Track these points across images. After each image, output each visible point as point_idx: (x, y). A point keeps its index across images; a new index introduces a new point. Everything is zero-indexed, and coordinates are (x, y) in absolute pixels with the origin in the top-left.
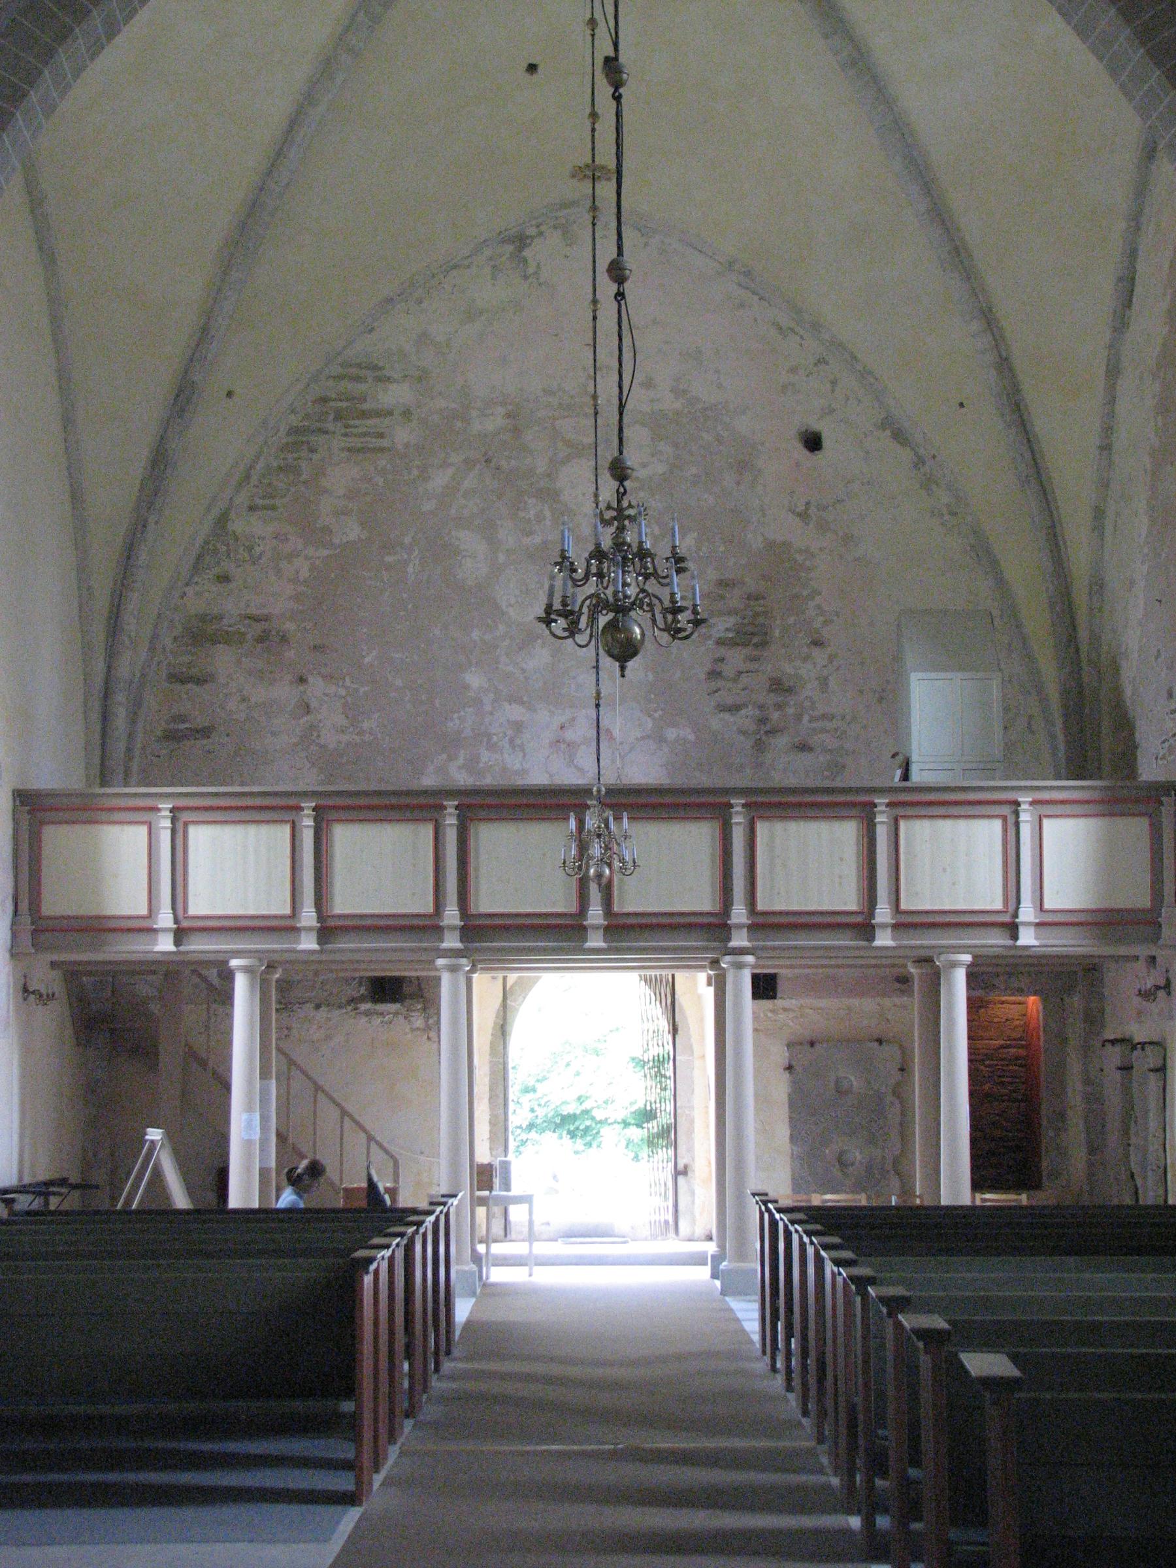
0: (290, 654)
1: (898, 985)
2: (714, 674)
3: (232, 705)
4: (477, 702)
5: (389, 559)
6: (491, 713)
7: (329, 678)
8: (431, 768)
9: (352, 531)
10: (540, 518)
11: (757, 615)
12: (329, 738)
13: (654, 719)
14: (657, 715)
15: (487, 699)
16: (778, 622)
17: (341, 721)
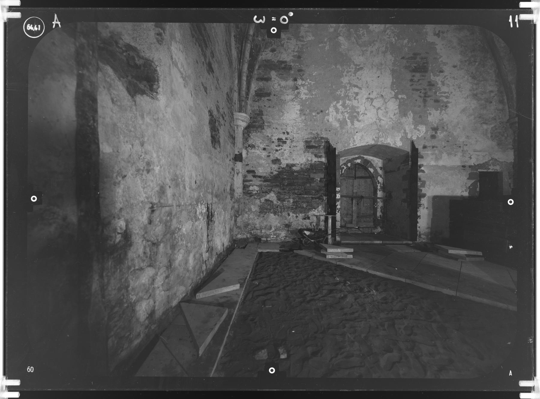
0: (292, 72)
1: (463, 168)
2: (411, 80)
3: (276, 86)
4: (346, 87)
5: (320, 45)
6: (349, 90)
7: (303, 80)
8: (332, 105)
9: (310, 38)
10: (363, 34)
11: (424, 63)
12: (303, 97)
13: (395, 92)
14: (396, 91)
15: (348, 86)
16: (430, 65)
17: (306, 91)
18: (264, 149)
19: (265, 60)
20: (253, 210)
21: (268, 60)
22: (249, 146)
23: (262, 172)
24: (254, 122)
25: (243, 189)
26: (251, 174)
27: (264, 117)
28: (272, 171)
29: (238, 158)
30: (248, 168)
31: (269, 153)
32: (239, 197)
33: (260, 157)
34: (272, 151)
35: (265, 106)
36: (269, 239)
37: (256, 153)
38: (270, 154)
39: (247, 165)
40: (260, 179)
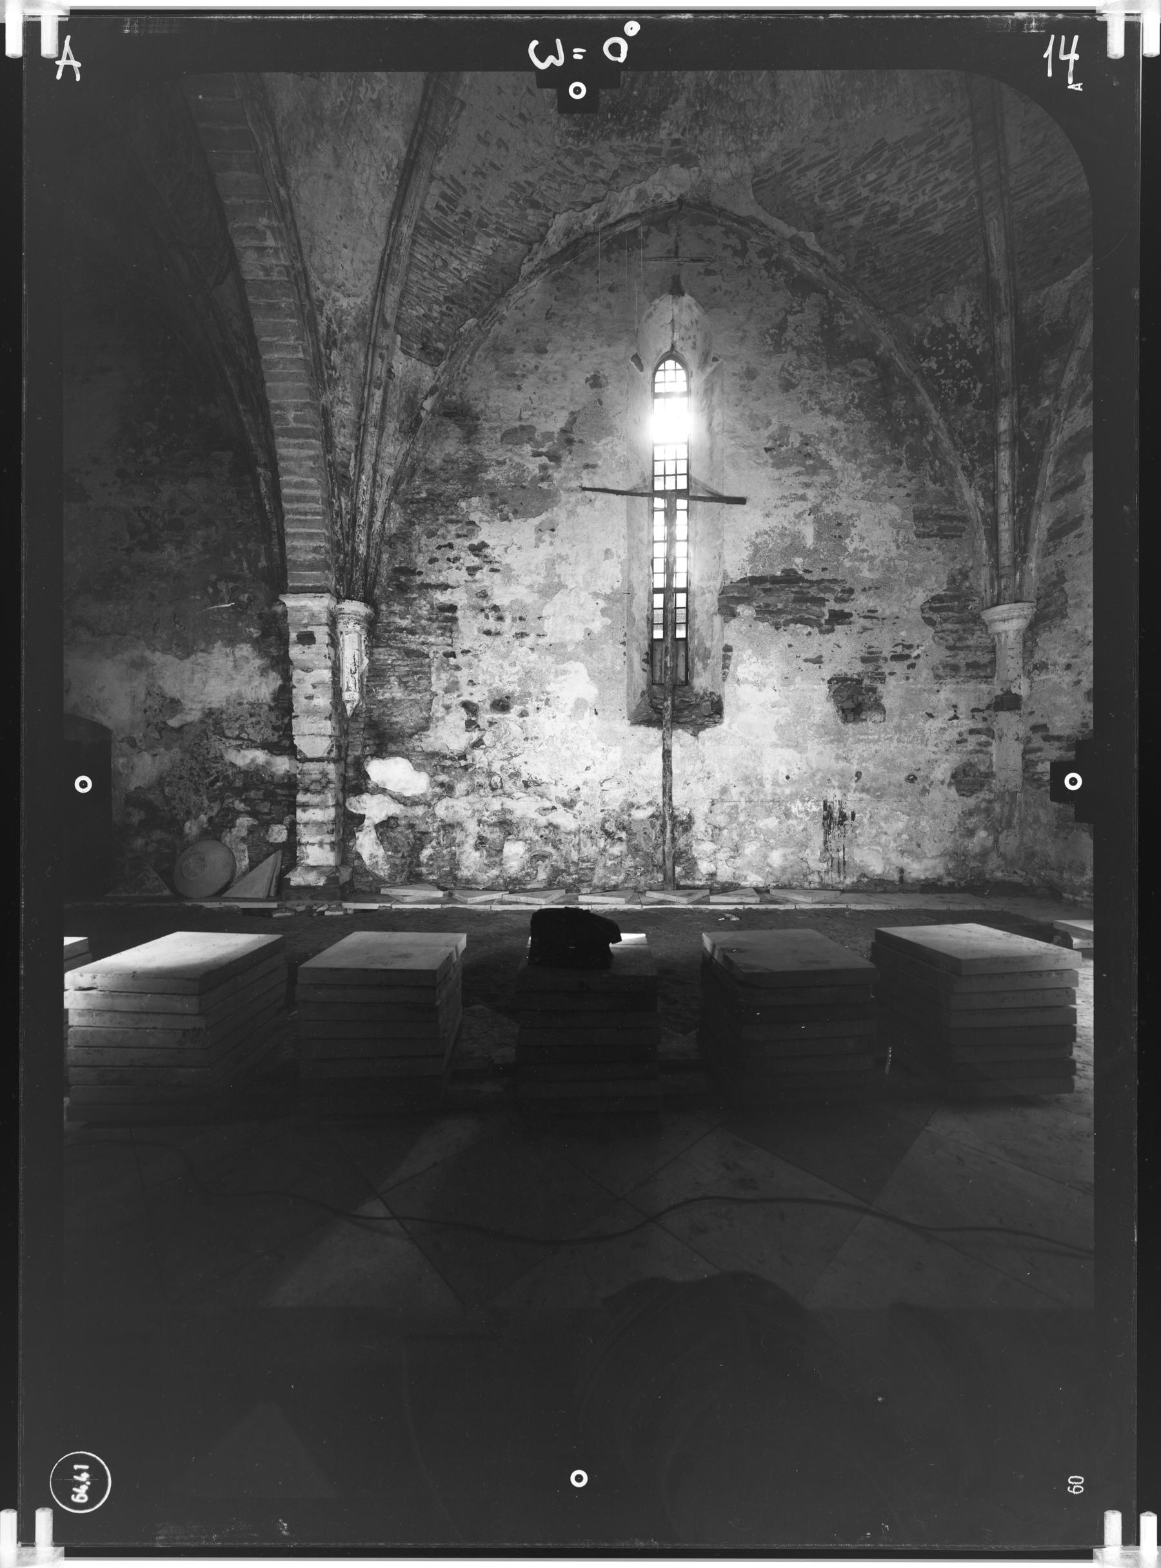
18: (1068, 667)
19: (1071, 439)
20: (1044, 819)
21: (1078, 433)
22: (1035, 667)
23: (1062, 726)
24: (1048, 605)
25: (1024, 771)
26: (1040, 733)
27: (1066, 586)
28: (1085, 721)
29: (1008, 702)
30: (1033, 721)
31: (1079, 674)
32: (1002, 790)
33: (1057, 690)
34: (1085, 669)
35: (1070, 556)
36: (1079, 899)
37: (1050, 680)
38: (1080, 677)
39: (1032, 713)
40: (1057, 744)
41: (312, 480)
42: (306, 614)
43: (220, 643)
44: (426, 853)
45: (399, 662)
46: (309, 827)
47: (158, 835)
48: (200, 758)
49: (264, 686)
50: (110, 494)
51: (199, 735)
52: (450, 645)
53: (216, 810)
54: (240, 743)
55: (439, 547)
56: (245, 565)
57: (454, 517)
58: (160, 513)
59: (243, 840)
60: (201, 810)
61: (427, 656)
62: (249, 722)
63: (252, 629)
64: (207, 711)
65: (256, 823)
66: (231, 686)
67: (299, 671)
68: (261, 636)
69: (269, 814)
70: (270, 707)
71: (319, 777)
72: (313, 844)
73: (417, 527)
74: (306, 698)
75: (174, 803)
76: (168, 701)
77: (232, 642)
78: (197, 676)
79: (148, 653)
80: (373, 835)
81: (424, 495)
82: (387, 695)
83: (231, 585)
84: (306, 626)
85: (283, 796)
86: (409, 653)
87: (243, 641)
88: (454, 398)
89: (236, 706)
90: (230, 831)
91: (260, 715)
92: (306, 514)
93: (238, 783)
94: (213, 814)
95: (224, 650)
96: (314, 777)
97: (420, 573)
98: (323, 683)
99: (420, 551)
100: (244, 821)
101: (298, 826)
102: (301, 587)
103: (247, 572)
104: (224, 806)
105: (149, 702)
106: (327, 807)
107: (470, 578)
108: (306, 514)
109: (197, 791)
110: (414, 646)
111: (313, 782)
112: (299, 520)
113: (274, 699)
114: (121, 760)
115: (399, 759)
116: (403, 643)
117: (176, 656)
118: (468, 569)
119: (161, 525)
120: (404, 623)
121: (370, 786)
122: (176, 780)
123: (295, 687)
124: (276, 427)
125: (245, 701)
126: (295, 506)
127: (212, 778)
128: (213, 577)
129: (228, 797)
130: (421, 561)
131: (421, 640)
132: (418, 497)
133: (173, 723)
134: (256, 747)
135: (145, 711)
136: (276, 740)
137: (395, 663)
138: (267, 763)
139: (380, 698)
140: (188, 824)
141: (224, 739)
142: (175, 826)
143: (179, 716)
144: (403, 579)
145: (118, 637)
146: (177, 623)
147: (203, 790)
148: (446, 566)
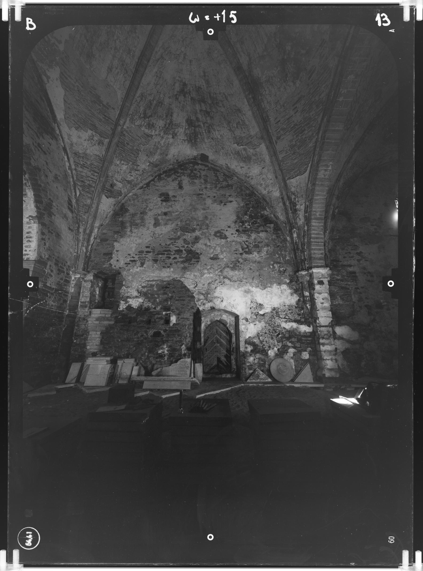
41: (321, 232)
42: (320, 274)
43: (275, 284)
44: (363, 363)
45: (339, 291)
46: (326, 352)
47: (258, 356)
48: (272, 326)
49: (292, 299)
50: (234, 237)
51: (271, 317)
52: (357, 285)
53: (280, 346)
54: (286, 320)
55: (346, 253)
56: (282, 259)
57: (349, 244)
58: (251, 242)
59: (292, 358)
60: (274, 346)
61: (349, 289)
62: (289, 312)
63: (286, 280)
64: (273, 308)
65: (296, 351)
66: (281, 299)
67: (317, 294)
68: (289, 282)
69: (300, 347)
70: (295, 307)
71: (327, 333)
72: (329, 360)
73: (338, 247)
74: (321, 303)
75: (264, 343)
76: (259, 304)
77: (279, 284)
78: (268, 296)
79: (250, 288)
80: (341, 356)
81: (338, 237)
82: (337, 303)
83: (279, 265)
84: (320, 278)
85: (305, 340)
86: (342, 288)
87: (284, 284)
88: (342, 209)
89: (283, 306)
90: (287, 354)
91: (292, 310)
92: (319, 242)
93: (287, 335)
94: (279, 347)
95: (277, 287)
96: (325, 333)
97: (341, 261)
98: (326, 298)
99: (340, 254)
100: (292, 351)
101: (322, 353)
102: (317, 266)
103: (282, 261)
104: (283, 344)
105: (252, 305)
106: (332, 345)
107: (359, 263)
108: (319, 242)
109: (272, 338)
110: (343, 286)
111: (325, 335)
112: (317, 244)
113: (297, 304)
114: (243, 326)
115: (346, 326)
116: (339, 284)
117: (261, 289)
118: (357, 260)
119: (252, 246)
120: (339, 278)
121: (337, 337)
122: (264, 334)
123: (316, 299)
124: (313, 217)
125: (286, 305)
126: (316, 240)
127: (277, 333)
128: (272, 263)
129: (284, 341)
130: (340, 257)
131: (345, 283)
132: (336, 238)
133: (261, 312)
134: (292, 322)
135: (251, 308)
136: (299, 319)
137: (338, 291)
138: (297, 328)
139: (335, 303)
140: (269, 352)
141: (280, 319)
142: (264, 352)
143: (263, 310)
144: (335, 263)
145: (239, 282)
146: (260, 277)
147: (274, 338)
148: (349, 259)
